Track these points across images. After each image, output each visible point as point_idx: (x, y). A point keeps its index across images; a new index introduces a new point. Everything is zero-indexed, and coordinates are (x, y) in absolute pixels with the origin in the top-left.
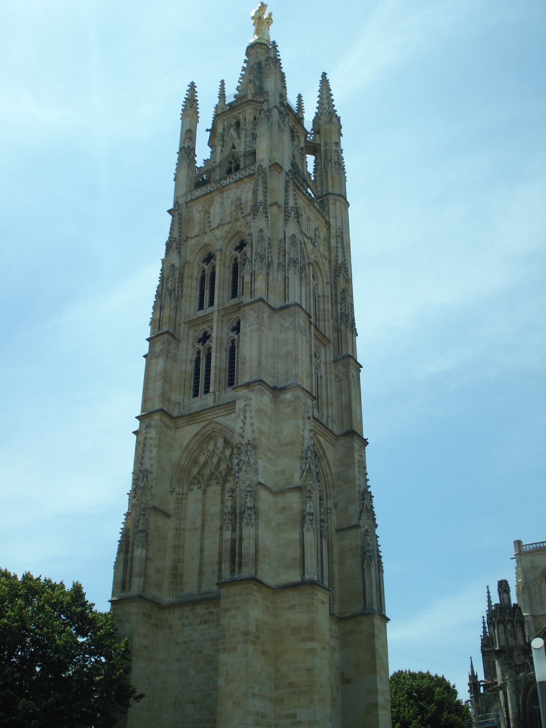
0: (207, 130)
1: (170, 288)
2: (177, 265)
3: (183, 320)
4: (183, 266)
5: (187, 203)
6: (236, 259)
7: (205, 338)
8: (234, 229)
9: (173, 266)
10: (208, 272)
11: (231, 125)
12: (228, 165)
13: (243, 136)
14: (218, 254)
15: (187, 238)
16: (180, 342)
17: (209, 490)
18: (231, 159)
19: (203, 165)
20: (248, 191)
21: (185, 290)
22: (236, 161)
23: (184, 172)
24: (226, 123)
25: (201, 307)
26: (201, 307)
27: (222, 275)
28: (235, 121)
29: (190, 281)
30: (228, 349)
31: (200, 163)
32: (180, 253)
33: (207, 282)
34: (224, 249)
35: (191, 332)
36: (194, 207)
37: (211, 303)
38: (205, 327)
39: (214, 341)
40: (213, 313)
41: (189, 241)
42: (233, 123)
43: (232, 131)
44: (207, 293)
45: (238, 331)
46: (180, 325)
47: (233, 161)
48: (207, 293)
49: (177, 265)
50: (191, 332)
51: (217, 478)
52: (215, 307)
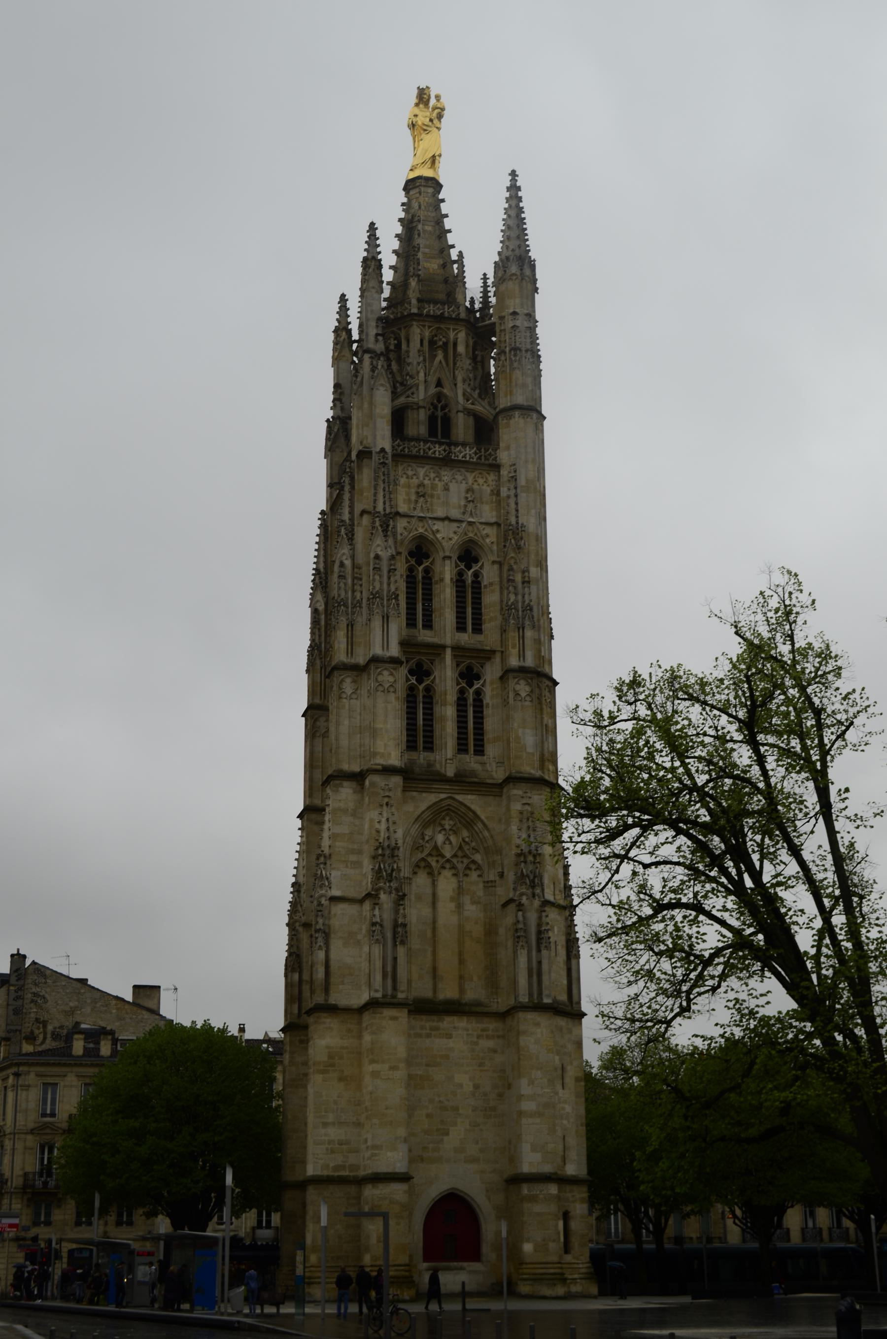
7: (420, 672)
15: (398, 514)
22: (443, 408)
24: (427, 333)
43: (440, 356)
47: (439, 405)
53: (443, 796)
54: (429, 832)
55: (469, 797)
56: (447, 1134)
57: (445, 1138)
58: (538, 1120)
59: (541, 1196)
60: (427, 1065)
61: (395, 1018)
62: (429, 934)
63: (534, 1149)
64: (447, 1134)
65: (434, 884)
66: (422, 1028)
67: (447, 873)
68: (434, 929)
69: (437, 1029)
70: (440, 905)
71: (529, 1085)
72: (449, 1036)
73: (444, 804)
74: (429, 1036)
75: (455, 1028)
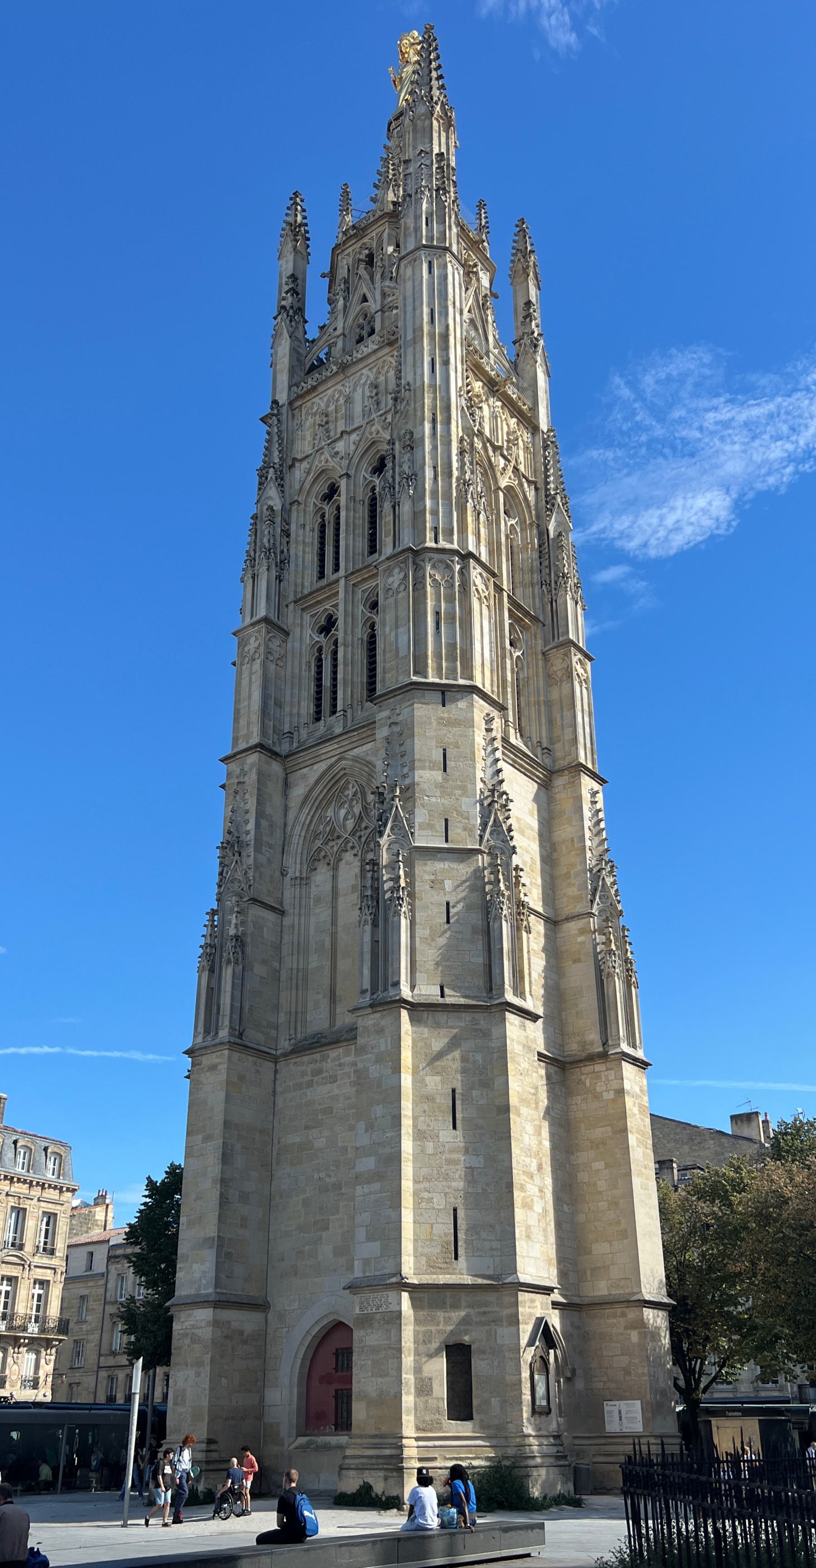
0: (323, 276)
1: (267, 545)
2: (278, 507)
3: (291, 598)
5: (291, 403)
7: (328, 626)
8: (367, 438)
9: (271, 508)
10: (329, 518)
11: (359, 260)
12: (358, 330)
13: (378, 277)
14: (343, 483)
16: (287, 634)
17: (342, 865)
18: (361, 321)
20: (387, 372)
21: (292, 546)
23: (284, 347)
25: (322, 575)
26: (322, 575)
27: (352, 518)
28: (367, 252)
29: (301, 532)
30: (365, 639)
32: (282, 486)
33: (327, 534)
34: (352, 472)
35: (307, 617)
36: (303, 407)
37: (337, 568)
38: (327, 607)
40: (337, 581)
41: (297, 464)
42: (362, 257)
46: (287, 606)
49: (278, 507)
50: (307, 617)
51: (353, 848)
52: (342, 572)
53: (334, 759)
54: (330, 813)
55: (365, 748)
56: (327, 1228)
57: (324, 1234)
58: (376, 1186)
59: (378, 1316)
60: (307, 1128)
61: (213, 1068)
63: (370, 1238)
64: (327, 1228)
65: (334, 877)
66: (303, 1074)
67: (348, 856)
68: (334, 935)
69: (319, 1072)
70: (341, 900)
71: (366, 1131)
72: (334, 1079)
73: (336, 769)
74: (310, 1084)
75: (340, 1065)
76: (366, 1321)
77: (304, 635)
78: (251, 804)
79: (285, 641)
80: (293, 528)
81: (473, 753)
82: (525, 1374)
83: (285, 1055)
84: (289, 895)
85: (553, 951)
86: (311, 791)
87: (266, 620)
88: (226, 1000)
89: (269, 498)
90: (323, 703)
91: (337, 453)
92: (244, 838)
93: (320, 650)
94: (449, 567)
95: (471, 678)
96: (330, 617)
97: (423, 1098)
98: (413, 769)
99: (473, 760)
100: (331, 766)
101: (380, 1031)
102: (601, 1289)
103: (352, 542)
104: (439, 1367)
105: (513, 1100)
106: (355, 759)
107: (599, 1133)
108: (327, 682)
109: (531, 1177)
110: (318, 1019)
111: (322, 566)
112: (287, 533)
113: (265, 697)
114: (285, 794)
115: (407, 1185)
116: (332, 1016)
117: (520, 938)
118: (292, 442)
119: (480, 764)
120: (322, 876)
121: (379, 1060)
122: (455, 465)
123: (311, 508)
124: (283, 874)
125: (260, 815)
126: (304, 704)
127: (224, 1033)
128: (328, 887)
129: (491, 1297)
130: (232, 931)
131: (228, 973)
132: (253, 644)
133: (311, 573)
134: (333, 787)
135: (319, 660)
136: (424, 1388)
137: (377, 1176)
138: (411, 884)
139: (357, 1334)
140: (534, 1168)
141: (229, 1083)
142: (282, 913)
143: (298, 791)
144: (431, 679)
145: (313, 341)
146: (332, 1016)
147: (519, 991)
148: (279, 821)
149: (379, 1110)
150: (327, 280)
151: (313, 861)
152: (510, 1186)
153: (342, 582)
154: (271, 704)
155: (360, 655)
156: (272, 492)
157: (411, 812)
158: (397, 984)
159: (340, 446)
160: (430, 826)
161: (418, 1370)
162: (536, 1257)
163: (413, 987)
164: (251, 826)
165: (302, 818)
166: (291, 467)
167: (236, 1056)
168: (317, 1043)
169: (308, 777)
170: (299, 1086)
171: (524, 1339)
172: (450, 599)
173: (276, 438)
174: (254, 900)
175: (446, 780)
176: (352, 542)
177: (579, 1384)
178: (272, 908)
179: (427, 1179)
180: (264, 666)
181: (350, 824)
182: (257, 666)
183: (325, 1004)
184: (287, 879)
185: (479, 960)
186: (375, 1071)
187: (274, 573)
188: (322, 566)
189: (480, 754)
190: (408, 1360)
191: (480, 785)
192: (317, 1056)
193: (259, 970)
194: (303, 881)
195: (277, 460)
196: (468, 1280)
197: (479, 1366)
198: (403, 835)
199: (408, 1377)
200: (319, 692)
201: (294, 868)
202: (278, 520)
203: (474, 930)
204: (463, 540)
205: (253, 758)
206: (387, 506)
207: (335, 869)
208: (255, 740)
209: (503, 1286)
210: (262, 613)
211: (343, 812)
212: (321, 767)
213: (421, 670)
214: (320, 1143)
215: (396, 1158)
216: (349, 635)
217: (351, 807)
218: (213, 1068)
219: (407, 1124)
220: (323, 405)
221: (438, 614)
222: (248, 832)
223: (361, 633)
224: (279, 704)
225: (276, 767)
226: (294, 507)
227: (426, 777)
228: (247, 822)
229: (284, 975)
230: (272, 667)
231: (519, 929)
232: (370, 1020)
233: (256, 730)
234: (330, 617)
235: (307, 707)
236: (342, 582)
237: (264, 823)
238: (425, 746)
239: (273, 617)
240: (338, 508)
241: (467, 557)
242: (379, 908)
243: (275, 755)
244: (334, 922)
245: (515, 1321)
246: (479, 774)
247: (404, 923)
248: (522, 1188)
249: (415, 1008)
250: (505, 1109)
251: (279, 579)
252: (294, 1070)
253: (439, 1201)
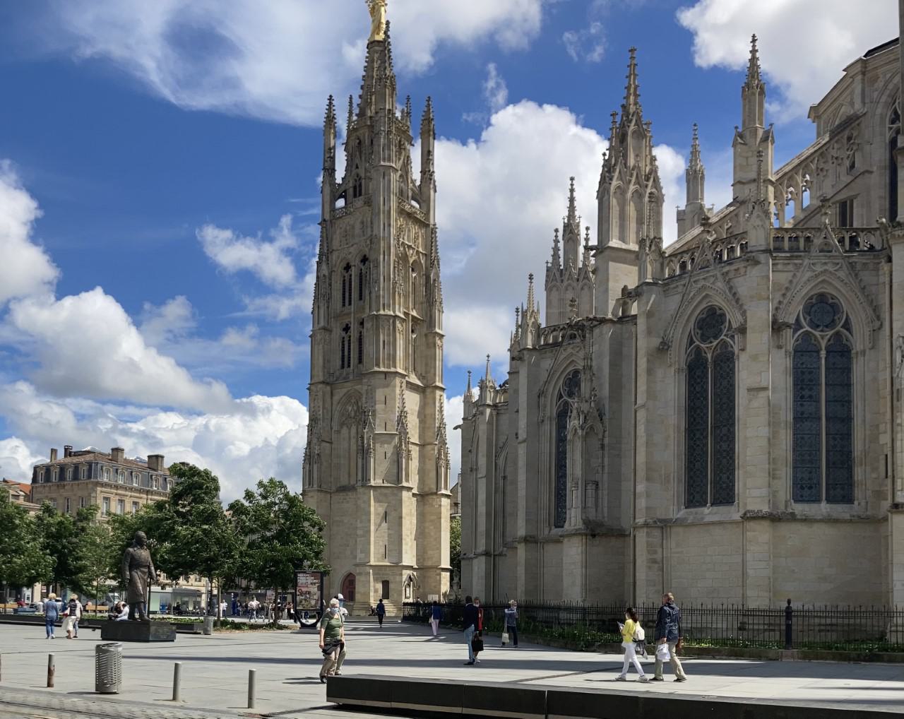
2: (327, 274)
4: (330, 274)
6: (361, 270)
7: (347, 329)
9: (324, 276)
14: (353, 268)
19: (341, 182)
25: (344, 305)
26: (344, 305)
31: (339, 180)
37: (350, 304)
39: (352, 332)
40: (350, 313)
44: (347, 294)
45: (363, 328)
48: (347, 294)
49: (327, 274)
60: (342, 516)
61: (312, 497)
62: (347, 456)
63: (361, 553)
72: (348, 502)
74: (343, 502)
76: (360, 574)
77: (338, 332)
78: (321, 404)
79: (331, 334)
80: (333, 282)
81: (395, 397)
82: (404, 588)
83: (334, 492)
84: (334, 436)
85: (422, 457)
86: (341, 398)
87: (324, 329)
88: (315, 476)
89: (323, 270)
90: (345, 362)
91: (350, 253)
92: (319, 417)
93: (344, 338)
94: (389, 321)
95: (395, 367)
96: (347, 325)
97: (377, 514)
98: (375, 404)
99: (395, 400)
100: (348, 391)
101: (364, 494)
102: (429, 563)
103: (355, 295)
104: (380, 586)
105: (404, 515)
106: (356, 390)
107: (433, 517)
108: (346, 353)
109: (408, 536)
110: (344, 481)
111: (344, 303)
112: (330, 285)
113: (324, 360)
114: (332, 398)
115: (372, 539)
116: (349, 480)
117: (408, 463)
118: (332, 239)
119: (398, 401)
120: (345, 431)
121: (364, 502)
122: (392, 276)
123: (339, 274)
124: (331, 428)
125: (324, 408)
126: (338, 361)
127: (315, 486)
128: (347, 435)
129: (395, 568)
130: (316, 452)
131: (315, 467)
132: (319, 337)
133: (339, 304)
134: (348, 396)
135: (343, 341)
136: (376, 591)
137: (363, 536)
138: (374, 446)
139: (357, 577)
140: (409, 534)
141: (317, 502)
142: (331, 443)
143: (336, 398)
144: (382, 369)
145: (339, 184)
146: (349, 480)
147: (407, 480)
148: (329, 408)
149: (364, 517)
150: (344, 146)
151: (342, 425)
152: (402, 539)
153: (352, 315)
154: (326, 361)
155: (357, 344)
156: (324, 266)
157: (375, 420)
158: (370, 480)
159: (352, 250)
160: (380, 425)
161: (374, 587)
162: (409, 558)
163: (374, 480)
164: (321, 412)
165: (338, 409)
166: (331, 252)
167: (319, 493)
168: (343, 489)
169: (340, 393)
170: (339, 503)
171: (404, 580)
172: (389, 335)
173: (325, 239)
174: (323, 441)
175: (386, 408)
176: (355, 295)
177: (421, 590)
178: (328, 442)
179: (377, 537)
180: (323, 347)
181: (353, 413)
182: (321, 347)
183: (346, 476)
184: (333, 430)
185: (395, 471)
186: (362, 505)
187: (326, 305)
188: (344, 303)
189: (398, 397)
190: (372, 584)
191: (397, 409)
192: (345, 494)
193: (325, 464)
194: (338, 432)
195: (326, 251)
196: (388, 564)
197: (391, 586)
198: (372, 429)
199: (372, 588)
200: (343, 356)
201: (335, 428)
202: (327, 280)
203: (394, 462)
204: (394, 312)
205: (320, 386)
206: (367, 292)
207: (350, 429)
208: (321, 379)
209: (398, 566)
210: (322, 324)
211: (350, 408)
212: (345, 390)
213: (378, 365)
214: (346, 521)
215: (369, 531)
216: (354, 333)
217: (353, 406)
218: (312, 497)
219: (372, 521)
220: (345, 226)
221: (384, 341)
222: (320, 415)
223: (357, 335)
224: (329, 361)
225: (329, 388)
226: (333, 273)
227: (379, 407)
228: (319, 411)
229: (333, 465)
230: (326, 346)
231: (408, 459)
232: (361, 490)
233: (321, 374)
234: (347, 325)
235: (339, 363)
236: (352, 315)
237: (325, 411)
238: (380, 394)
239: (326, 326)
240: (351, 275)
241: (396, 317)
242: (364, 452)
243: (328, 384)
244: (350, 449)
245: (401, 575)
246: (398, 405)
247: (372, 460)
248: (405, 540)
249: (375, 488)
250: (401, 518)
251: (328, 307)
252: (336, 498)
253: (381, 543)
